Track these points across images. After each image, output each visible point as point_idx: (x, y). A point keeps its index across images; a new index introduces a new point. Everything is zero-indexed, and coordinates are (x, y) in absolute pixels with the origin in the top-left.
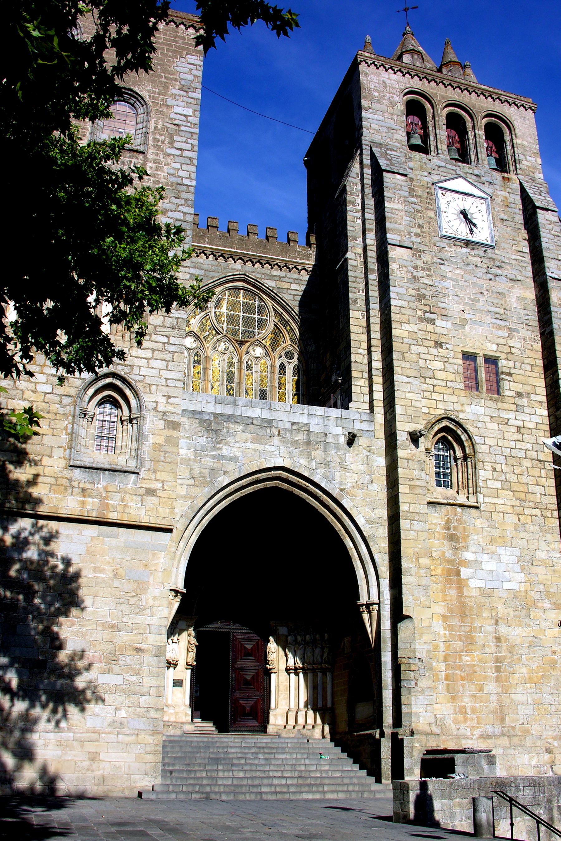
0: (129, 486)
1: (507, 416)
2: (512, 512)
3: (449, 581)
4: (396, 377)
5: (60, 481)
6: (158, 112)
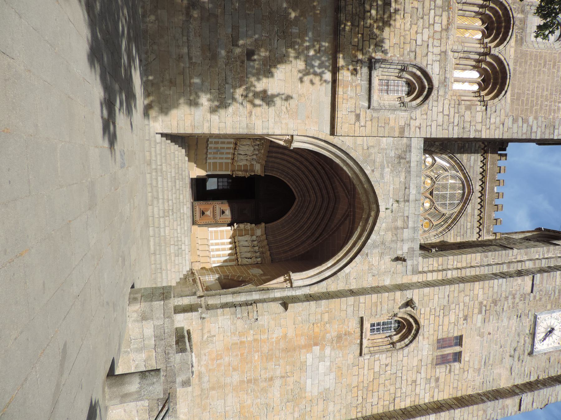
0: (361, 103)
1: (422, 372)
2: (359, 381)
4: (448, 287)
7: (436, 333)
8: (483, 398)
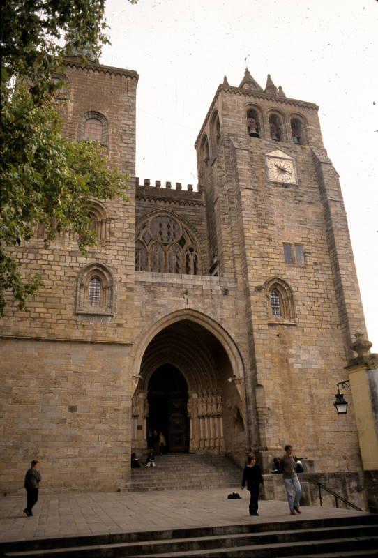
3: (282, 366)
4: (248, 258)
5: (71, 322)
6: (113, 123)
7: (281, 264)
8: (330, 228)
